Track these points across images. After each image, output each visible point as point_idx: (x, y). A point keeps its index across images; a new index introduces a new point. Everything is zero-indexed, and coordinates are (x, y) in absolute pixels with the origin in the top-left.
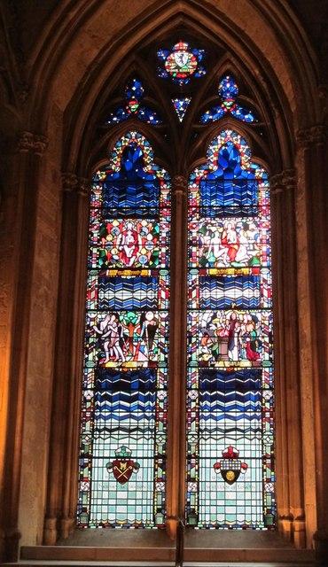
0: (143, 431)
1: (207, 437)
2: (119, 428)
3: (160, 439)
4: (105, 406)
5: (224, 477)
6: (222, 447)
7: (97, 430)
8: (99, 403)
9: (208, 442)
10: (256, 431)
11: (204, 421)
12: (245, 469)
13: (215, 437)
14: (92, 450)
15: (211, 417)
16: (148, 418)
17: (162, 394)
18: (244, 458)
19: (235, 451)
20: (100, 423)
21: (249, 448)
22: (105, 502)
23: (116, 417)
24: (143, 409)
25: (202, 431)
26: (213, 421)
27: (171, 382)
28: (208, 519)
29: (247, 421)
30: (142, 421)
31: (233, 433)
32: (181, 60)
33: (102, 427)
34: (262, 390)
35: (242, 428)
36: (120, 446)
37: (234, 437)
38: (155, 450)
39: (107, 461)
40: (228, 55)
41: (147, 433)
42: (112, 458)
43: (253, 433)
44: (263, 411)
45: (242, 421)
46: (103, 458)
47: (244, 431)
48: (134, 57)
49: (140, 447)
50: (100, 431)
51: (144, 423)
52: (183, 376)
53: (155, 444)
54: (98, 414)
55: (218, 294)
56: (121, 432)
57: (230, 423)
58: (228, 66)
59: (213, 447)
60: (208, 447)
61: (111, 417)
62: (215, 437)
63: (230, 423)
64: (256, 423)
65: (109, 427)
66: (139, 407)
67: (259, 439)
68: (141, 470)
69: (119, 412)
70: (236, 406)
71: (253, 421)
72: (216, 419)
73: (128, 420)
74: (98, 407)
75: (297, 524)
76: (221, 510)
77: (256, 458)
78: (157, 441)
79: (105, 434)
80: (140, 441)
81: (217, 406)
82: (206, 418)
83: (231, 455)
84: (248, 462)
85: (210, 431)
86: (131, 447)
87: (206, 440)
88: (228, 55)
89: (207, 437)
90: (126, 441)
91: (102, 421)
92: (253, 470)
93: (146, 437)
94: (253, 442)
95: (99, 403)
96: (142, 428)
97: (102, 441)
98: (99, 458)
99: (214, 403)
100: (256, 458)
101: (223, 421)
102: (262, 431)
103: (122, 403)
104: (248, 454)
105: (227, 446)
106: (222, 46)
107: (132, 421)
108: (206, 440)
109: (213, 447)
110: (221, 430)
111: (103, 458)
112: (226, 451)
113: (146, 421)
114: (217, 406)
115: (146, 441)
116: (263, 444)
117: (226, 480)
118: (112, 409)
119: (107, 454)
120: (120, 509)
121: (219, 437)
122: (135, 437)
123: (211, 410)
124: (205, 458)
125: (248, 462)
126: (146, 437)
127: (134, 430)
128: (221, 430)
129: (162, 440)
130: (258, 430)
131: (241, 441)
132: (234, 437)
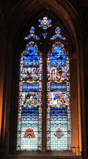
0: (35, 124)
2: (28, 124)
3: (40, 126)
4: (24, 118)
6: (57, 129)
7: (22, 124)
8: (23, 117)
10: (65, 124)
14: (21, 130)
15: (53, 120)
16: (36, 121)
17: (40, 114)
18: (63, 132)
19: (60, 130)
20: (23, 122)
21: (64, 129)
22: (24, 143)
23: (27, 120)
24: (35, 118)
25: (51, 124)
27: (43, 111)
29: (63, 121)
30: (34, 121)
31: (60, 125)
32: (45, 22)
34: (68, 113)
35: (62, 123)
40: (58, 21)
41: (36, 125)
43: (65, 125)
44: (68, 119)
45: (62, 121)
47: (62, 124)
49: (34, 129)
50: (23, 124)
51: (35, 122)
52: (46, 110)
55: (55, 87)
56: (29, 125)
57: (59, 122)
59: (54, 129)
60: (53, 129)
61: (26, 120)
63: (59, 122)
64: (66, 122)
66: (34, 118)
71: (65, 121)
73: (30, 121)
75: (77, 149)
76: (56, 145)
77: (66, 132)
80: (35, 127)
81: (55, 118)
82: (52, 121)
83: (59, 131)
85: (53, 124)
90: (30, 127)
91: (24, 121)
95: (23, 117)
96: (35, 123)
99: (54, 117)
100: (66, 132)
102: (67, 124)
103: (29, 117)
104: (63, 131)
109: (54, 129)
110: (56, 124)
112: (58, 130)
113: (36, 121)
114: (55, 118)
115: (36, 127)
118: (26, 118)
122: (33, 126)
123: (53, 118)
124: (52, 132)
127: (32, 124)
129: (40, 127)
130: (66, 124)
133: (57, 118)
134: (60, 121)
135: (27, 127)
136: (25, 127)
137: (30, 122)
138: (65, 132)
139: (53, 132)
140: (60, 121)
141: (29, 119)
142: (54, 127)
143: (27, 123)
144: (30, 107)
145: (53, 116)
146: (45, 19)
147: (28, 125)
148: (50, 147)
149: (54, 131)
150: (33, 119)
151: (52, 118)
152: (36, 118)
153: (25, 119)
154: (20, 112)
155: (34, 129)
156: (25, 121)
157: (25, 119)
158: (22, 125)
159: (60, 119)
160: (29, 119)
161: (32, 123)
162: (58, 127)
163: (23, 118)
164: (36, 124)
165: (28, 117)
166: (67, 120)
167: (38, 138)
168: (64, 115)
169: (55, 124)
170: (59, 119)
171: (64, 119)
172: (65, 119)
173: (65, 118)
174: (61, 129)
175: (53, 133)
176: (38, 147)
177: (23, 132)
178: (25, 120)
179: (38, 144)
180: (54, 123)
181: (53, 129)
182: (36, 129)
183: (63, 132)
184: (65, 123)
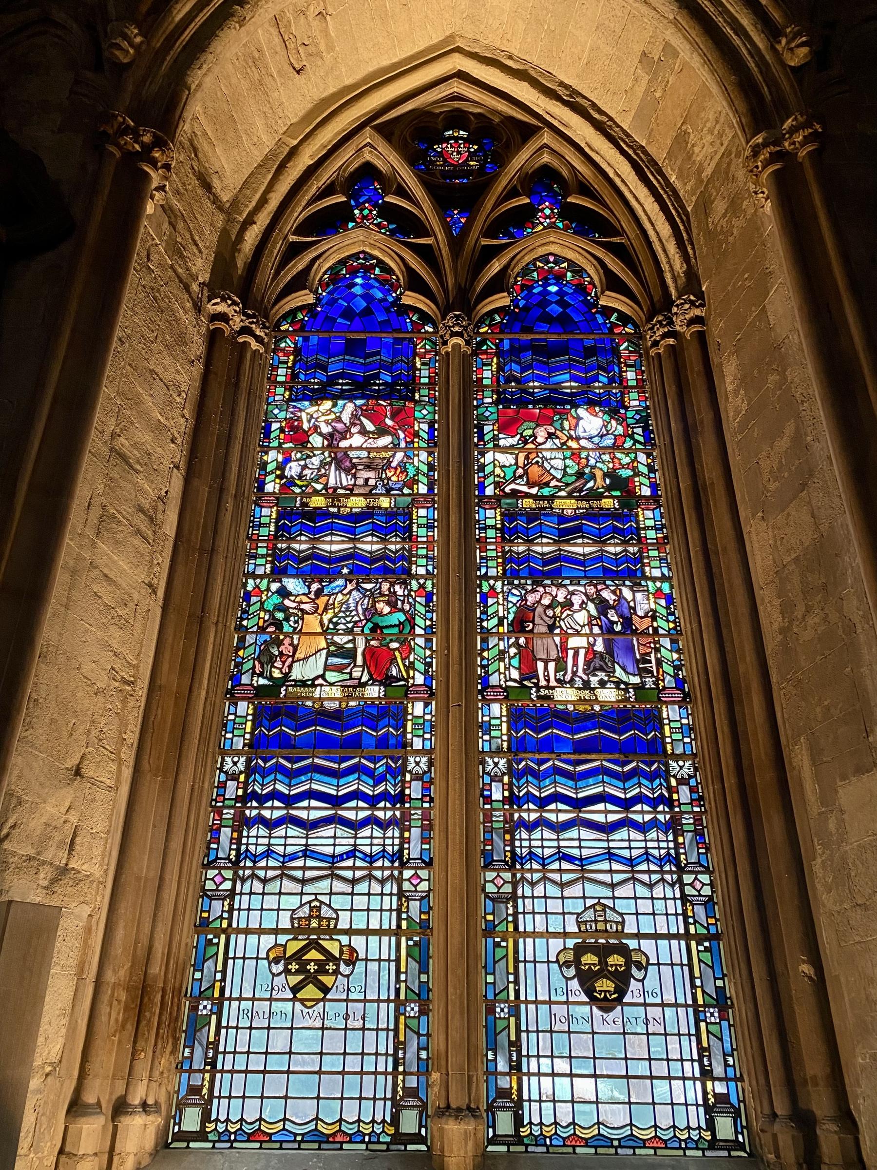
0: (371, 858)
1: (537, 876)
2: (307, 853)
5: (590, 992)
9: (539, 891)
10: (661, 861)
11: (525, 836)
12: (639, 966)
13: (556, 877)
16: (383, 825)
18: (638, 936)
24: (373, 801)
26: (548, 834)
28: (548, 1119)
29: (635, 835)
30: (366, 832)
33: (261, 849)
35: (626, 853)
37: (606, 878)
38: (399, 911)
40: (546, 138)
42: (285, 931)
43: (653, 867)
45: (623, 833)
46: (260, 931)
47: (631, 862)
48: (368, 136)
50: (255, 858)
53: (401, 894)
54: (254, 813)
56: (310, 863)
59: (554, 906)
62: (556, 877)
67: (672, 885)
68: (360, 967)
71: (653, 835)
73: (329, 831)
74: (254, 796)
78: (406, 886)
80: (362, 887)
82: (531, 827)
86: (338, 902)
87: (533, 884)
88: (546, 138)
89: (537, 876)
90: (324, 886)
91: (263, 831)
92: (666, 970)
93: (378, 874)
94: (658, 892)
97: (258, 887)
98: (247, 931)
101: (573, 833)
102: (677, 861)
105: (589, 903)
108: (533, 884)
109: (554, 906)
111: (260, 931)
115: (376, 888)
116: (684, 898)
117: (593, 1000)
120: (298, 1086)
121: (566, 877)
122: (348, 874)
123: (542, 803)
125: (647, 946)
126: (378, 874)
128: (570, 859)
132: (606, 878)
133: (578, 804)
134: (608, 828)
135: (289, 886)
138: (656, 936)
140: (608, 828)
141: (314, 803)
142: (553, 891)
144: (327, 704)
146: (457, 139)
148: (519, 1104)
149: (555, 925)
150: (353, 804)
151: (530, 798)
152: (385, 796)
153: (274, 811)
154: (239, 744)
155: (360, 902)
156: (271, 825)
157: (277, 803)
158: (249, 864)
159: (600, 806)
160: (317, 811)
162: (592, 890)
163: (262, 799)
164: (383, 854)
165: (311, 794)
166: (674, 826)
167: (399, 1004)
170: (597, 813)
171: (641, 814)
172: (646, 808)
173: (654, 803)
174: (621, 906)
176: (395, 1104)
178: (277, 814)
179: (395, 1073)
182: (375, 903)
183: (638, 936)
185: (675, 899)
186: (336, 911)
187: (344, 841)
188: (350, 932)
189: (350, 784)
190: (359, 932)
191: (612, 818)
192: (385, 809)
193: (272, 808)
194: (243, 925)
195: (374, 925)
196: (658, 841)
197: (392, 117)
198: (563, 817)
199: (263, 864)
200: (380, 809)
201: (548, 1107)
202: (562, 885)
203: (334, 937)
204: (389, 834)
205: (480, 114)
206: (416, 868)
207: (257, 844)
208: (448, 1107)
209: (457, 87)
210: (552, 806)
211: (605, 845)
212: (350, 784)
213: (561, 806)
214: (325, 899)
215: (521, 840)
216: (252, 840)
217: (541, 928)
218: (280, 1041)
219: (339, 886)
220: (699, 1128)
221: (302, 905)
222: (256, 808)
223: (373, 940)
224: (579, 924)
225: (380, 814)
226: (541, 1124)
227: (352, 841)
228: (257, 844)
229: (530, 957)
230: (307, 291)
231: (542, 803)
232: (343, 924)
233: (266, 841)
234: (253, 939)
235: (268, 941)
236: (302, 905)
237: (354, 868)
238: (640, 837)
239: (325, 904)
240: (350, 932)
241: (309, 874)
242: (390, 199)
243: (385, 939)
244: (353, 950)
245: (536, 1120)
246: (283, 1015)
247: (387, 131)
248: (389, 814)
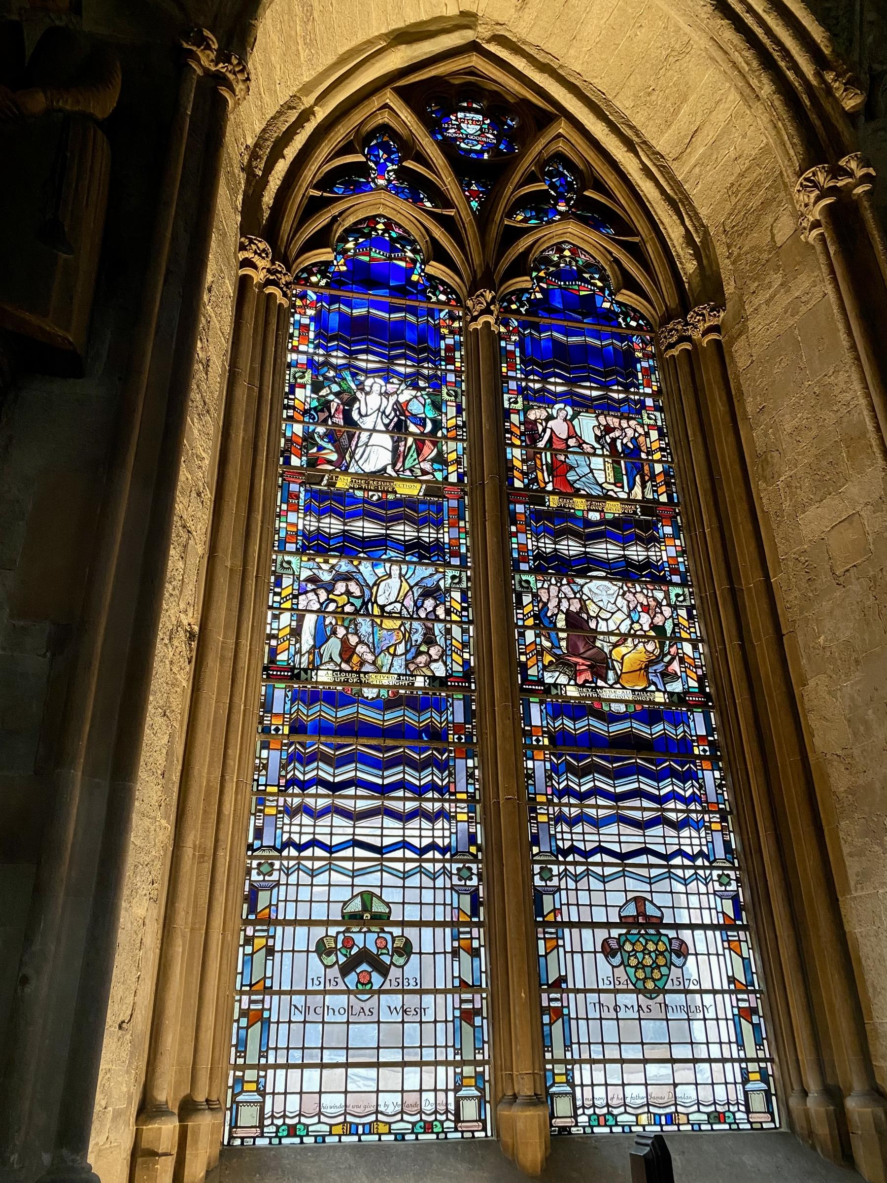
1: (580, 869)
4: (319, 782)
6: (618, 899)
10: (693, 858)
15: (581, 818)
16: (432, 817)
19: (651, 911)
24: (419, 792)
26: (588, 828)
31: (642, 859)
33: (305, 839)
35: (661, 849)
36: (357, 890)
39: (319, 932)
40: (563, 127)
42: (336, 923)
45: (658, 830)
46: (310, 923)
50: (301, 848)
56: (360, 853)
58: (561, 146)
63: (632, 839)
65: (326, 840)
68: (414, 958)
69: (356, 797)
70: (638, 793)
71: (685, 833)
72: (597, 823)
73: (376, 821)
79: (313, 858)
80: (414, 881)
82: (572, 822)
84: (686, 935)
85: (586, 854)
86: (389, 895)
88: (563, 127)
90: (373, 879)
93: (428, 866)
94: (693, 887)
96: (415, 842)
105: (630, 895)
106: (550, 108)
107: (389, 822)
111: (310, 923)
114: (596, 792)
115: (427, 882)
119: (319, 912)
121: (608, 871)
124: (580, 925)
127: (394, 847)
130: (701, 854)
131: (664, 885)
132: (644, 872)
135: (336, 878)
136: (323, 878)
137: (367, 831)
139: (593, 925)
141: (361, 792)
142: (595, 884)
143: (336, 840)
145: (581, 773)
147: (348, 853)
152: (432, 786)
155: (412, 895)
157: (322, 791)
158: (294, 852)
159: (636, 803)
161: (387, 841)
162: (631, 884)
163: (304, 785)
168: (670, 773)
169: (601, 850)
171: (674, 810)
174: (658, 899)
175: (588, 946)
177: (295, 923)
180: (590, 846)
181: (584, 898)
182: (428, 896)
184: (688, 850)
185: (708, 894)
186: (387, 904)
187: (340, 831)
188: (403, 924)
189: (393, 776)
190: (412, 924)
191: (648, 815)
192: (433, 800)
193: (317, 796)
194: (290, 916)
195: (428, 916)
196: (691, 838)
197: (417, 79)
198: (602, 813)
199: (308, 853)
200: (428, 800)
201: (600, 1092)
202: (603, 879)
203: (386, 929)
204: (439, 825)
205: (496, 92)
206: (464, 862)
207: (300, 833)
208: (515, 1096)
209: (475, 61)
210: (592, 801)
211: (642, 839)
212: (393, 776)
213: (601, 802)
214: (377, 891)
215: (562, 832)
216: (295, 829)
217: (586, 918)
218: (335, 1035)
219: (388, 879)
220: (738, 1103)
221: (353, 897)
222: (297, 795)
223: (427, 932)
224: (620, 917)
225: (428, 806)
226: (594, 1106)
227: (401, 832)
228: (300, 833)
229: (577, 948)
230: (329, 250)
231: (582, 797)
232: (396, 916)
233: (311, 830)
234: (302, 931)
235: (319, 932)
236: (353, 897)
237: (405, 860)
238: (673, 833)
239: (376, 896)
240: (403, 924)
241: (358, 865)
242: (409, 164)
243: (439, 931)
244: (408, 943)
245: (588, 1103)
246: (605, 1008)
247: (404, 94)
248: (438, 805)
